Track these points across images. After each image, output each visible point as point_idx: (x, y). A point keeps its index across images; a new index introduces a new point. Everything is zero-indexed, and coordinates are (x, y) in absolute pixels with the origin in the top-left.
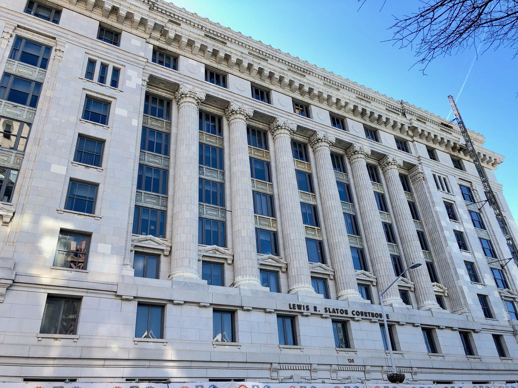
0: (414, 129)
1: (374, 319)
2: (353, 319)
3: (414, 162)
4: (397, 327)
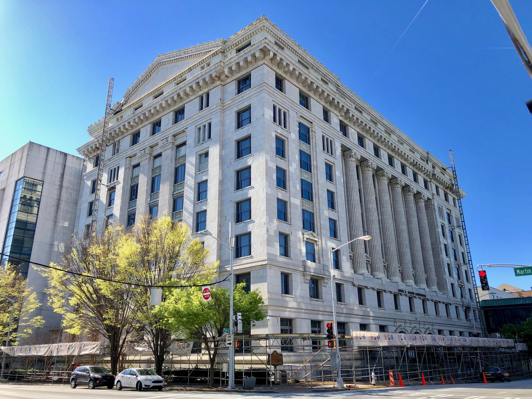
0: (434, 175)
1: (422, 297)
2: (415, 297)
3: (431, 197)
4: (450, 306)
